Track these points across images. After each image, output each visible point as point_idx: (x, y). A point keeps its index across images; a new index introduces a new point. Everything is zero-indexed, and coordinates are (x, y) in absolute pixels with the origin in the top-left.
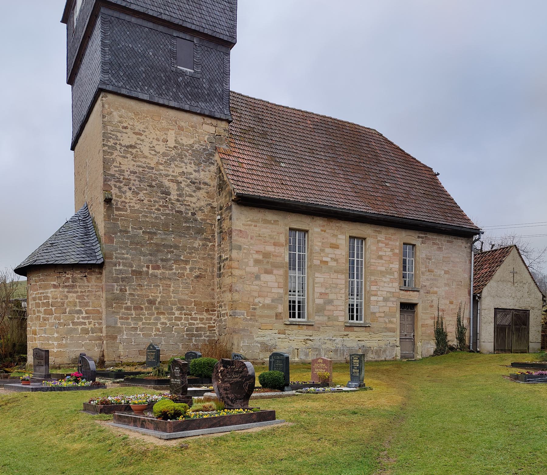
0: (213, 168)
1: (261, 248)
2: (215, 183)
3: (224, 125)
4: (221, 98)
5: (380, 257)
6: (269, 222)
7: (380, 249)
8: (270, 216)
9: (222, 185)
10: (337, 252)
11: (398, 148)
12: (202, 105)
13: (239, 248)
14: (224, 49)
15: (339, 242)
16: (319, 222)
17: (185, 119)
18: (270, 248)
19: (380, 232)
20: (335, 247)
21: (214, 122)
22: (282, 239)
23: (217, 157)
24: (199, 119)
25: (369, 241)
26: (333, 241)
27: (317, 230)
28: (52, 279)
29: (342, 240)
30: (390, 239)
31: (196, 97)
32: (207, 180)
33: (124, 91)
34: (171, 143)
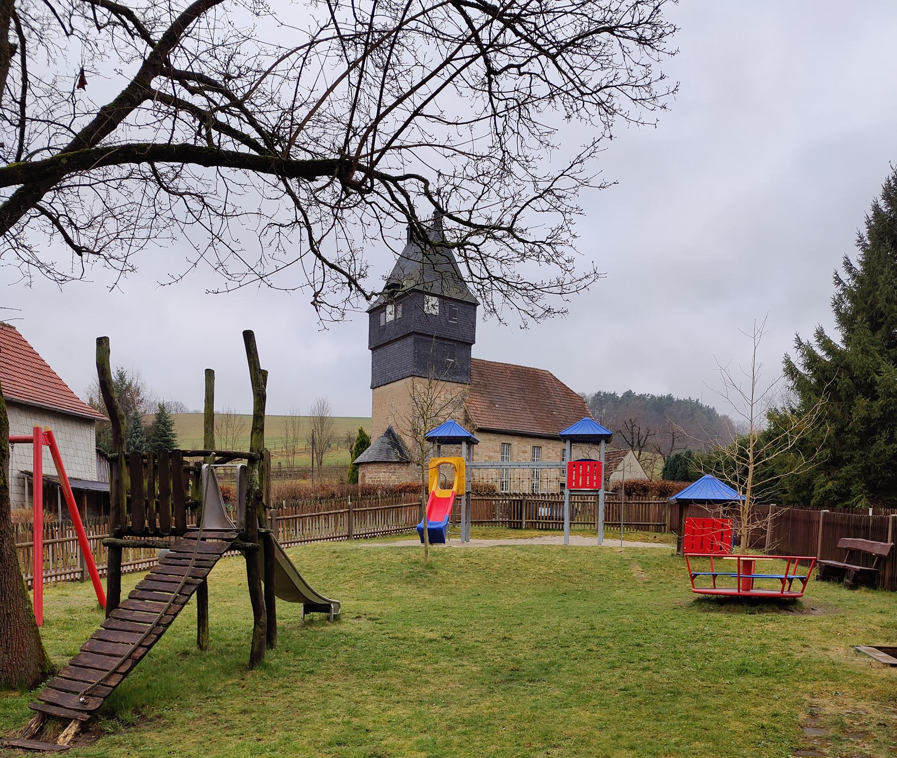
0: (462, 410)
1: (487, 454)
2: (463, 418)
3: (468, 387)
4: (467, 373)
5: (549, 457)
6: (492, 440)
7: (549, 453)
8: (492, 437)
9: (467, 420)
10: (526, 455)
11: (562, 384)
12: (458, 377)
13: (477, 454)
14: (468, 347)
15: (527, 449)
16: (517, 439)
17: (449, 385)
18: (492, 454)
19: (549, 444)
20: (525, 452)
21: (463, 385)
22: (498, 449)
23: (464, 404)
24: (456, 384)
25: (543, 448)
26: (524, 449)
27: (516, 443)
28: (383, 468)
29: (529, 448)
30: (555, 447)
31: (455, 374)
32: (459, 417)
33: (423, 375)
34: (442, 399)
